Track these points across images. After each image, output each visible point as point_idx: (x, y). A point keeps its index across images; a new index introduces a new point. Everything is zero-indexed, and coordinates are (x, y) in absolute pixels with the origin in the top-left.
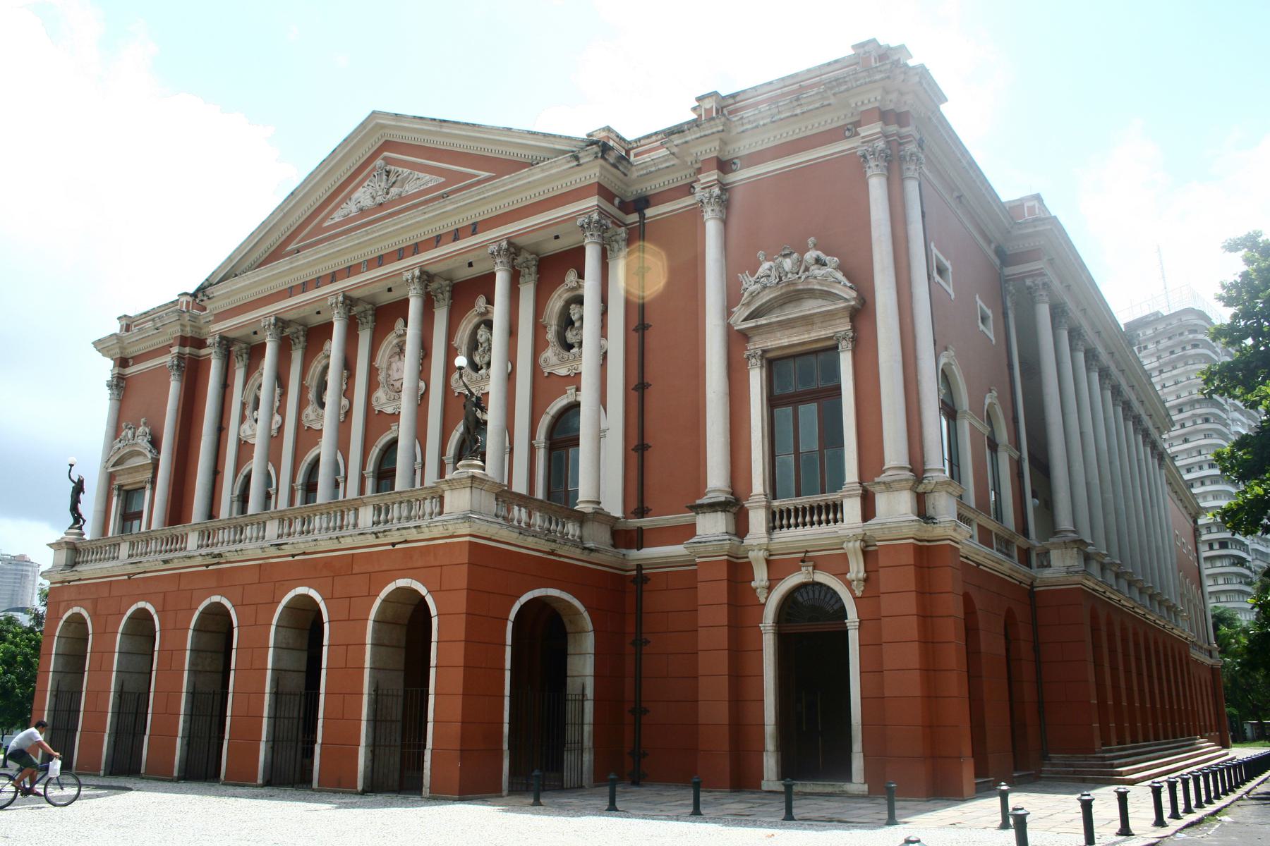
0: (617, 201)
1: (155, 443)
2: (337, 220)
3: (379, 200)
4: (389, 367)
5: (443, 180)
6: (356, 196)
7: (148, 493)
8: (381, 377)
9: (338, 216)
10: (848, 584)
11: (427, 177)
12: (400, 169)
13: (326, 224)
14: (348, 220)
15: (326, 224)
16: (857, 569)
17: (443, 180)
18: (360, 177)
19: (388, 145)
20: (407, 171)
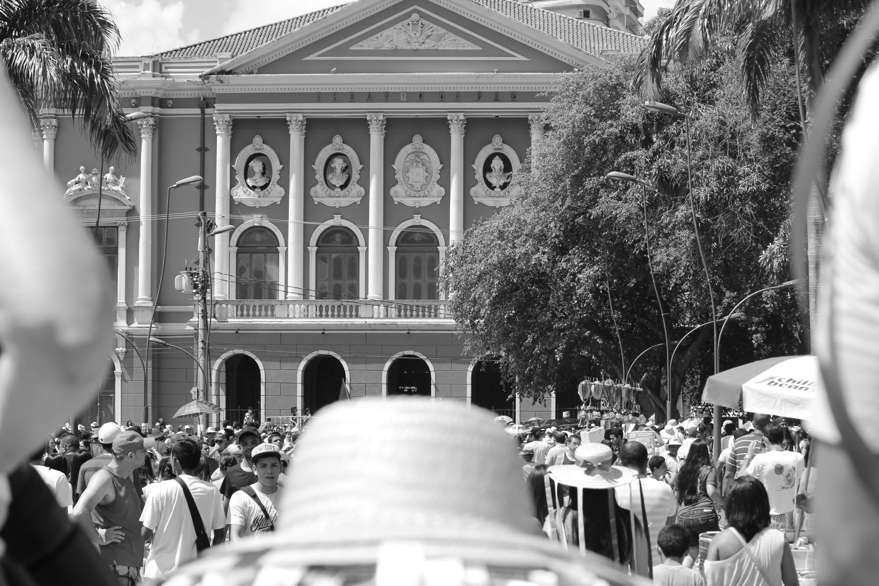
2: (366, 48)
4: (406, 171)
5: (479, 48)
7: (122, 236)
8: (399, 176)
12: (435, 27)
13: (353, 48)
15: (353, 48)
17: (479, 48)
20: (442, 31)
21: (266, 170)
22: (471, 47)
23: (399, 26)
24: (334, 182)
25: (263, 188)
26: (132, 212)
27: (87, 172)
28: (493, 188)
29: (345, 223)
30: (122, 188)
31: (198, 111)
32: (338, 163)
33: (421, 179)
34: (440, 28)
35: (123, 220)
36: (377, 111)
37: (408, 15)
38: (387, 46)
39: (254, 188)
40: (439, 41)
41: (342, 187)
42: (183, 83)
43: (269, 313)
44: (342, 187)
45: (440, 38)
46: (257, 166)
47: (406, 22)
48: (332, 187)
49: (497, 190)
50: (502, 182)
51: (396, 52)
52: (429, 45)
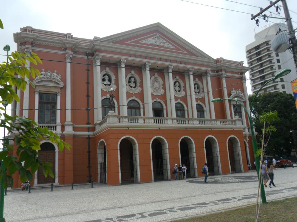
0: (215, 71)
1: (64, 80)
2: (144, 43)
3: (158, 44)
5: (175, 48)
6: (149, 39)
9: (144, 42)
10: (246, 140)
11: (171, 46)
12: (163, 40)
13: (140, 42)
14: (147, 44)
15: (140, 42)
16: (248, 139)
17: (175, 48)
18: (170, 41)
19: (157, 31)
20: (165, 41)
21: (110, 80)
22: (173, 47)
23: (153, 38)
24: (132, 85)
25: (109, 85)
26: (64, 88)
27: (45, 71)
28: (177, 91)
29: (136, 99)
30: (60, 79)
31: (86, 57)
32: (133, 80)
33: (158, 86)
34: (164, 40)
35: (59, 91)
36: (149, 62)
37: (156, 35)
38: (150, 43)
39: (106, 85)
40: (164, 44)
41: (135, 87)
42: (82, 46)
43: (137, 121)
44: (135, 87)
45: (164, 43)
46: (107, 78)
47: (155, 37)
48: (131, 87)
49: (178, 92)
50: (179, 90)
51: (152, 45)
52: (162, 44)
